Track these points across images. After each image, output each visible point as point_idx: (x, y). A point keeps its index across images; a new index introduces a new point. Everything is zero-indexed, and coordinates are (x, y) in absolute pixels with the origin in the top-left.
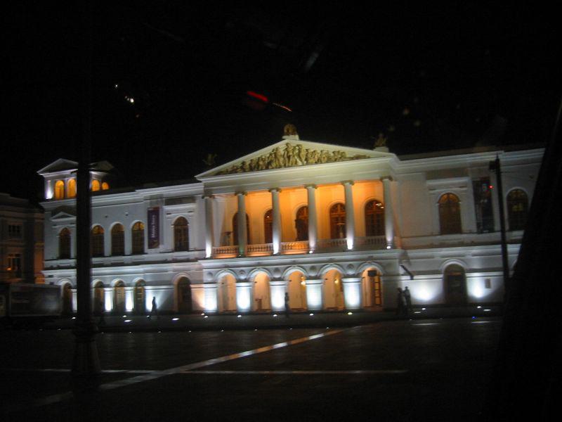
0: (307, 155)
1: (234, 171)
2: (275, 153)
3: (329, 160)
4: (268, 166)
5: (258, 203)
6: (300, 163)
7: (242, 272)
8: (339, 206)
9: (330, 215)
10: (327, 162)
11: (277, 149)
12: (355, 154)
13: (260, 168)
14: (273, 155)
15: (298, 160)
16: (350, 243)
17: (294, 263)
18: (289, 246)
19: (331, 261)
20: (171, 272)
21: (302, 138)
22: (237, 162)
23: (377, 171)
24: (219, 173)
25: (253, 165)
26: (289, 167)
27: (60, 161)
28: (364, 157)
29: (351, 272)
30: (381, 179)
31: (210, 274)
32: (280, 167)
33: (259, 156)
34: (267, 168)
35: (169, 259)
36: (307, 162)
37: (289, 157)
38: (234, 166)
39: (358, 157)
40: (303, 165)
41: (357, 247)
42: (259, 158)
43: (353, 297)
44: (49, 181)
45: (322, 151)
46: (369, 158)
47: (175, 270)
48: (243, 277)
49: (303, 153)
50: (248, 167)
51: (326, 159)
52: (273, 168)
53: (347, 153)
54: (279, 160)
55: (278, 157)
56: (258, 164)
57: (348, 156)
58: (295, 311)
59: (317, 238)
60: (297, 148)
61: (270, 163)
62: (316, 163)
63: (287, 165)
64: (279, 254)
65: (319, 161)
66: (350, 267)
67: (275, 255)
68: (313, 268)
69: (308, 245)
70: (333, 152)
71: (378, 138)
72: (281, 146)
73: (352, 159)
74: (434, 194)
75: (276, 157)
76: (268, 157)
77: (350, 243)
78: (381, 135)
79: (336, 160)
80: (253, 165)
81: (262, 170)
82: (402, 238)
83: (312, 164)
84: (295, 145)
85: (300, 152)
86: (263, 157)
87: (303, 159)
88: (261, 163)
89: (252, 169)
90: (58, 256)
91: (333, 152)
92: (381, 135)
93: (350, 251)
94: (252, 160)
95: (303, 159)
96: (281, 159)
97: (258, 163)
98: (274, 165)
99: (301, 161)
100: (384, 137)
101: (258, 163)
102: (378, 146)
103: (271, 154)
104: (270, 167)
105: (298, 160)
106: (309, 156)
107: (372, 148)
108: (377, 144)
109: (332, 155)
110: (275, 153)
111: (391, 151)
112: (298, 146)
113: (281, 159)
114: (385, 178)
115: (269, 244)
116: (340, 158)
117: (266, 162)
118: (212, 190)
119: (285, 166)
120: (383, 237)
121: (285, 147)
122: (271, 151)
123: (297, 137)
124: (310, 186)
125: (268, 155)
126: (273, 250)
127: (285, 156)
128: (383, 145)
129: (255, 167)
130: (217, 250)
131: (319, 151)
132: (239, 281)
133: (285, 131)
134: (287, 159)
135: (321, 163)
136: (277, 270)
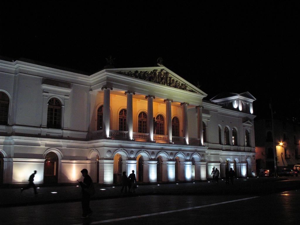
1: (129, 74)
3: (181, 88)
5: (118, 101)
7: (132, 152)
8: (124, 111)
10: (179, 88)
11: (156, 70)
16: (187, 141)
24: (120, 73)
31: (109, 151)
33: (146, 71)
35: (43, 134)
36: (170, 85)
38: (130, 71)
39: (192, 91)
42: (145, 72)
46: (196, 93)
47: (46, 145)
65: (175, 87)
68: (171, 154)
73: (190, 91)
79: (183, 89)
85: (167, 77)
89: (136, 77)
99: (167, 83)
103: (152, 72)
109: (181, 85)
118: (112, 84)
122: (152, 70)
125: (150, 72)
132: (130, 159)
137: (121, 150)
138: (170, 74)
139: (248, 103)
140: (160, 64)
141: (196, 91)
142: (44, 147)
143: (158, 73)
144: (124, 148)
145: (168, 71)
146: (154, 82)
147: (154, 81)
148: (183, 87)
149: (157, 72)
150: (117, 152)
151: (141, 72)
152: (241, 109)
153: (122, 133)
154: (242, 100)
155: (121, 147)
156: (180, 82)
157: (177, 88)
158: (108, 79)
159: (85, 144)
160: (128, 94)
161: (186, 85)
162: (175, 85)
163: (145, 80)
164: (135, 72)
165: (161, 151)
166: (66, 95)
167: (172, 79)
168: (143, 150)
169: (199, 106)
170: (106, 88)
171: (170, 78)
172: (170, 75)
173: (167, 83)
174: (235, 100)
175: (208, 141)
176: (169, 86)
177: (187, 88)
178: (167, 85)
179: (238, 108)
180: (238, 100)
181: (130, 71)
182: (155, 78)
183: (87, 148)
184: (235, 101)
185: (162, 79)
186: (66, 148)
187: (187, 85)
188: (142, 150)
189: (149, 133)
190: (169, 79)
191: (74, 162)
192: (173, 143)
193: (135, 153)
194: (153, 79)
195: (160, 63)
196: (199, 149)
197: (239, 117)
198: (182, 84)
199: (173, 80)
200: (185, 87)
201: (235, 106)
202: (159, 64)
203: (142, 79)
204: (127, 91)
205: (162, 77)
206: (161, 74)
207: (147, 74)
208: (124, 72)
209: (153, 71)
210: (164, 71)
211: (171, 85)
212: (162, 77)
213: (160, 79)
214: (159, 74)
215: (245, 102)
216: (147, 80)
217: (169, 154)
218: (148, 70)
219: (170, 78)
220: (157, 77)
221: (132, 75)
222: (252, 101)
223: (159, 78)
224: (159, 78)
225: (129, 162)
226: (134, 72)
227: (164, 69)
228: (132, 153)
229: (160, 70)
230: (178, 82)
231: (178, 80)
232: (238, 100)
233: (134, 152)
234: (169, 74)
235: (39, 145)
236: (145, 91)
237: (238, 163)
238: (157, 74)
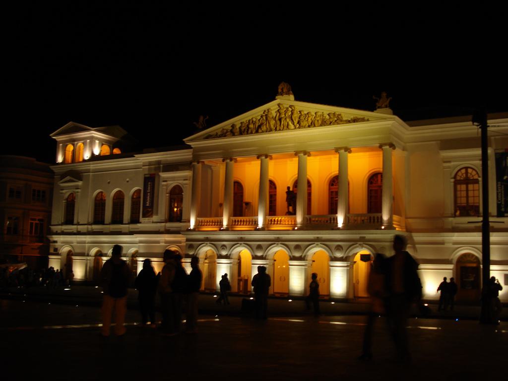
2: (266, 115)
3: (324, 123)
5: (249, 172)
6: (292, 126)
7: (224, 247)
9: (330, 189)
10: (321, 125)
12: (352, 117)
13: (250, 131)
14: (264, 118)
15: (290, 123)
16: (340, 220)
17: (277, 241)
19: (318, 240)
20: (163, 244)
21: (297, 99)
22: (227, 124)
23: (377, 136)
24: (208, 137)
25: (243, 129)
26: (280, 130)
27: (70, 124)
28: (363, 120)
29: (339, 255)
30: (381, 147)
32: (271, 130)
33: (250, 118)
34: (257, 132)
36: (300, 125)
37: (280, 120)
39: (355, 120)
40: (295, 128)
41: (348, 225)
42: (249, 121)
43: (338, 285)
44: (61, 145)
45: (316, 113)
46: (368, 120)
47: (166, 242)
48: (224, 253)
49: (296, 116)
50: (238, 130)
51: (320, 122)
52: (263, 132)
53: (343, 115)
54: (269, 123)
55: (269, 119)
56: (248, 127)
57: (344, 119)
58: (279, 295)
60: (290, 109)
61: (260, 127)
62: (309, 126)
63: (278, 128)
64: (263, 229)
65: (312, 125)
66: (339, 248)
67: (259, 230)
68: (297, 247)
69: (295, 221)
70: (329, 115)
71: (380, 98)
72: (272, 106)
73: (349, 122)
74: (449, 167)
75: (266, 118)
76: (259, 120)
77: (340, 220)
78: (384, 94)
79: (330, 124)
80: (243, 129)
81: (252, 133)
82: (407, 218)
83: (305, 127)
84: (288, 106)
86: (254, 120)
87: (296, 122)
88: (251, 126)
90: (92, 222)
91: (329, 115)
92: (384, 94)
93: (339, 229)
94: (241, 123)
95: (296, 122)
96: (273, 122)
97: (248, 126)
98: (264, 128)
100: (387, 97)
101: (248, 126)
102: (379, 108)
103: (262, 116)
104: (260, 131)
105: (290, 123)
106: (302, 118)
107: (372, 109)
108: (378, 105)
110: (266, 115)
111: (394, 114)
112: (291, 106)
113: (273, 122)
114: (385, 144)
116: (336, 121)
117: (257, 125)
119: (276, 130)
120: (379, 215)
121: (277, 108)
123: (292, 97)
124: (301, 153)
125: (259, 118)
126: (257, 225)
127: (277, 118)
128: (386, 107)
129: (245, 130)
130: (202, 222)
132: (221, 257)
133: (280, 91)
134: (278, 122)
135: (315, 126)
136: (259, 247)
142: (163, 244)
148: (338, 120)
153: (254, 220)
162: (311, 123)
163: (248, 133)
165: (275, 244)
166: (185, 180)
168: (241, 243)
171: (300, 112)
176: (299, 128)
188: (239, 243)
193: (345, 249)
196: (368, 236)
208: (215, 133)
217: (292, 248)
218: (254, 116)
228: (223, 248)
230: (319, 114)
233: (343, 248)
235: (158, 242)
236: (251, 150)
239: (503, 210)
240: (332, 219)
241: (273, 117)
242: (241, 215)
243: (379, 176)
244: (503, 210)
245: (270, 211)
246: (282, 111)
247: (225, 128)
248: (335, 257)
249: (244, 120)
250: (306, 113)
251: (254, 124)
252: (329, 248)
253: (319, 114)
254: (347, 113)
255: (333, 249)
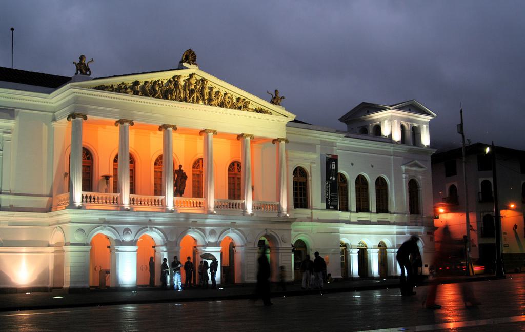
0: (210, 94)
4: (166, 94)
6: (201, 102)
7: (127, 231)
11: (179, 77)
18: (102, 198)
31: (81, 230)
34: (165, 97)
38: (123, 83)
39: (261, 111)
42: (155, 82)
46: (271, 114)
48: (128, 238)
59: (216, 196)
73: (256, 111)
79: (240, 108)
85: (203, 88)
97: (153, 87)
99: (203, 99)
103: (169, 81)
109: (235, 101)
112: (203, 80)
115: (161, 197)
125: (165, 81)
131: (222, 93)
137: (105, 227)
138: (209, 82)
139: (416, 125)
140: (188, 64)
141: (270, 111)
143: (184, 80)
144: (110, 224)
145: (204, 77)
146: (175, 99)
147: (174, 97)
148: (241, 105)
149: (182, 79)
150: (145, 231)
151: (146, 82)
152: (397, 137)
154: (400, 119)
155: (105, 222)
156: (232, 95)
157: (226, 107)
158: (76, 100)
159: (44, 217)
160: (119, 125)
161: (246, 100)
163: (153, 97)
164: (133, 82)
166: (4, 132)
167: (215, 90)
169: (278, 138)
170: (74, 118)
171: (211, 89)
172: (209, 84)
173: (203, 99)
174: (386, 118)
175: (312, 206)
177: (250, 106)
178: (205, 103)
179: (390, 136)
180: (391, 119)
181: (123, 83)
182: (176, 91)
183: (49, 226)
184: (386, 121)
185: (192, 92)
186: (7, 226)
187: (248, 100)
189: (165, 195)
190: (207, 91)
191: (24, 249)
192: (215, 212)
194: (171, 94)
195: (188, 63)
197: (395, 154)
198: (238, 99)
199: (218, 93)
200: (245, 103)
201: (385, 132)
202: (185, 64)
203: (149, 96)
204: (117, 120)
205: (193, 87)
206: (191, 84)
207: (159, 84)
209: (172, 78)
210: (196, 77)
211: (213, 103)
212: (193, 87)
213: (188, 92)
214: (186, 83)
215: (409, 123)
216: (158, 97)
219: (211, 89)
220: (181, 89)
221: (126, 89)
222: (427, 119)
223: (185, 90)
224: (185, 90)
225: (120, 249)
226: (132, 84)
227: (195, 74)
228: (127, 233)
229: (188, 75)
230: (228, 95)
231: (228, 91)
232: (391, 119)
234: (207, 82)
237: (391, 248)
238: (182, 83)
239: (329, 203)
240: (234, 205)
241: (181, 86)
242: (92, 191)
243: (201, 161)
244: (329, 203)
245: (296, 200)
246: (193, 81)
247: (125, 82)
248: (123, 240)
249: (149, 80)
250: (215, 90)
251: (160, 87)
252: (116, 231)
253: (228, 95)
254: (255, 101)
255: (207, 233)
